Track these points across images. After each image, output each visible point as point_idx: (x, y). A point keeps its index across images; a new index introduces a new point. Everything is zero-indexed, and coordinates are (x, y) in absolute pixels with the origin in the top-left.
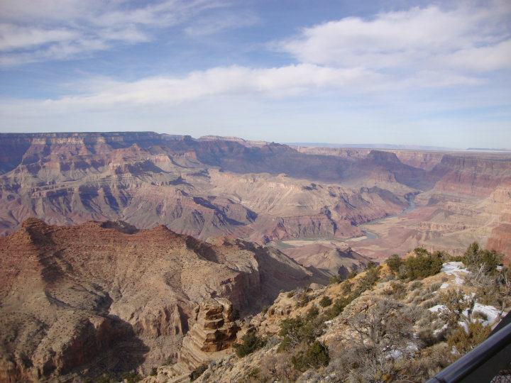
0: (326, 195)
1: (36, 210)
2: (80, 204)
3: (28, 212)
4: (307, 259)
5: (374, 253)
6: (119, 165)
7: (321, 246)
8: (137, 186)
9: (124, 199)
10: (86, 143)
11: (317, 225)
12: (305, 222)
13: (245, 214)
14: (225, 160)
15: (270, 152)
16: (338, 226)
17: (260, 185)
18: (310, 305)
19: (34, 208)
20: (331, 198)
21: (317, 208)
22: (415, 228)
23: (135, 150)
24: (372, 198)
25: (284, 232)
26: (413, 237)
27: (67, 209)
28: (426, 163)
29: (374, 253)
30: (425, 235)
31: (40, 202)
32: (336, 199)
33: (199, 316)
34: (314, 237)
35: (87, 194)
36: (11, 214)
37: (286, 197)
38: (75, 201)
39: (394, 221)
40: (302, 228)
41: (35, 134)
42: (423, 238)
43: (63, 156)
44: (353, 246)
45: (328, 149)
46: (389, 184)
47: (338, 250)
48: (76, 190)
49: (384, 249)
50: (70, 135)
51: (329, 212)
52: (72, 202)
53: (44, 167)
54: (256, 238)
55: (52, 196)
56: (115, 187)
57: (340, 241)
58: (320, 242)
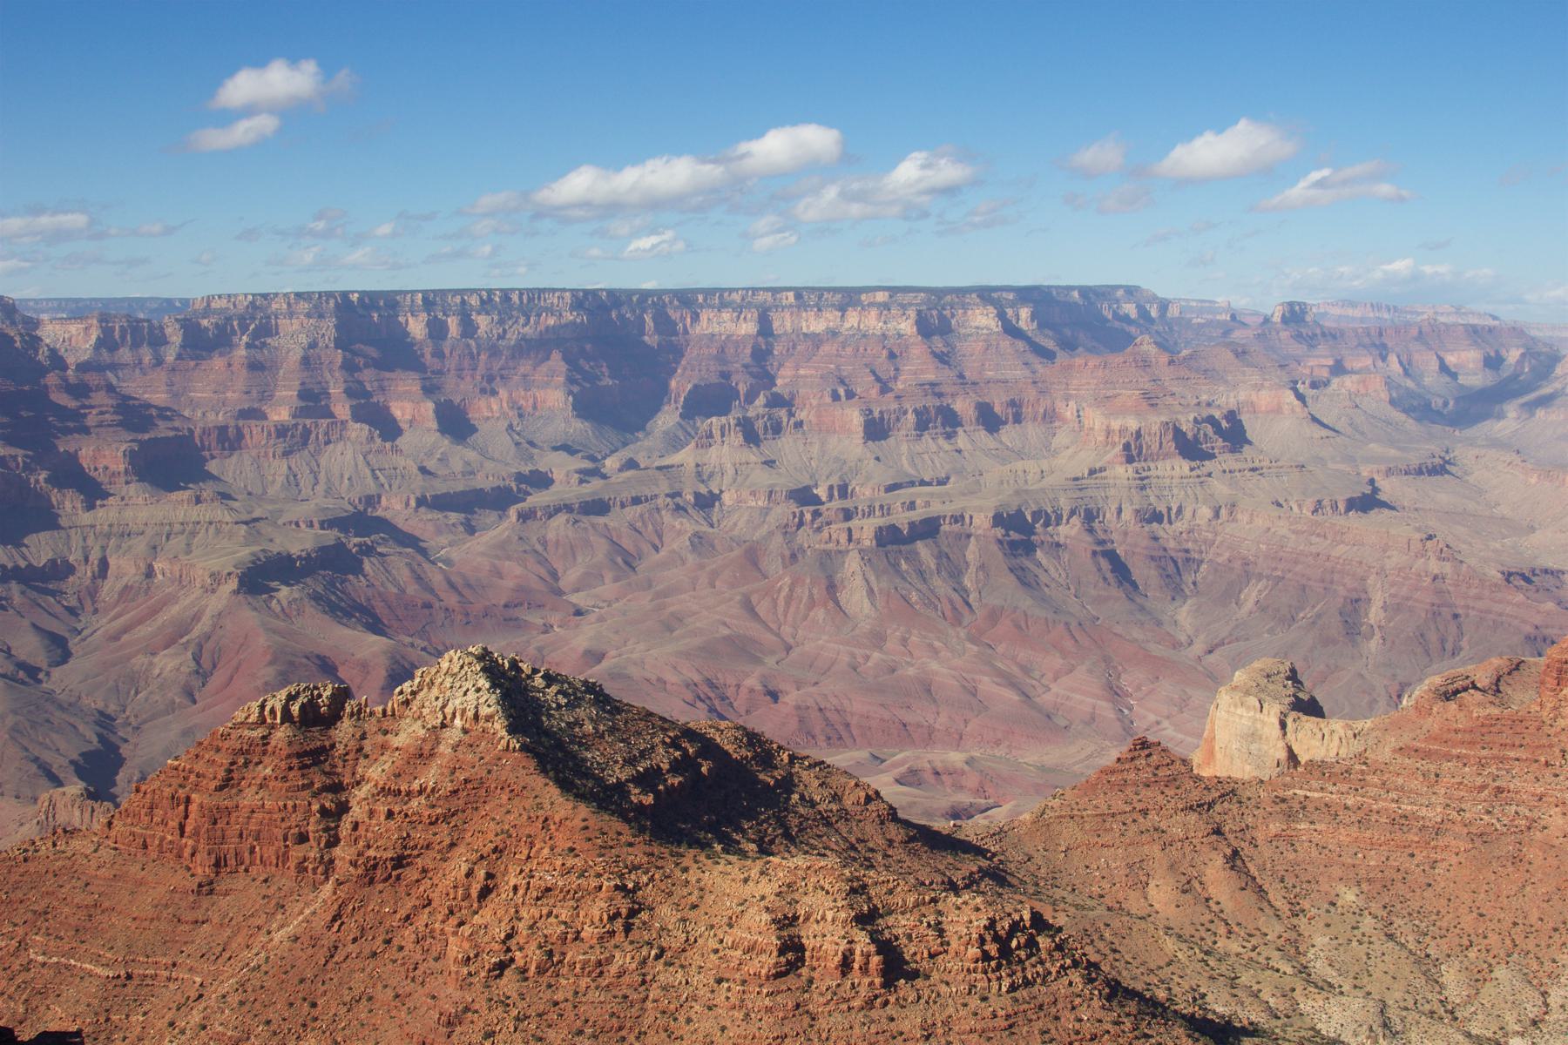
1: (843, 597)
2: (1010, 581)
3: (812, 604)
6: (1133, 424)
8: (1217, 515)
9: (1171, 569)
10: (925, 328)
19: (832, 588)
23: (1145, 364)
27: (955, 596)
31: (853, 563)
35: (1019, 532)
36: (749, 608)
38: (982, 567)
41: (709, 292)
43: (842, 382)
48: (981, 521)
50: (849, 298)
52: (972, 569)
53: (799, 425)
55: (889, 537)
56: (1127, 514)
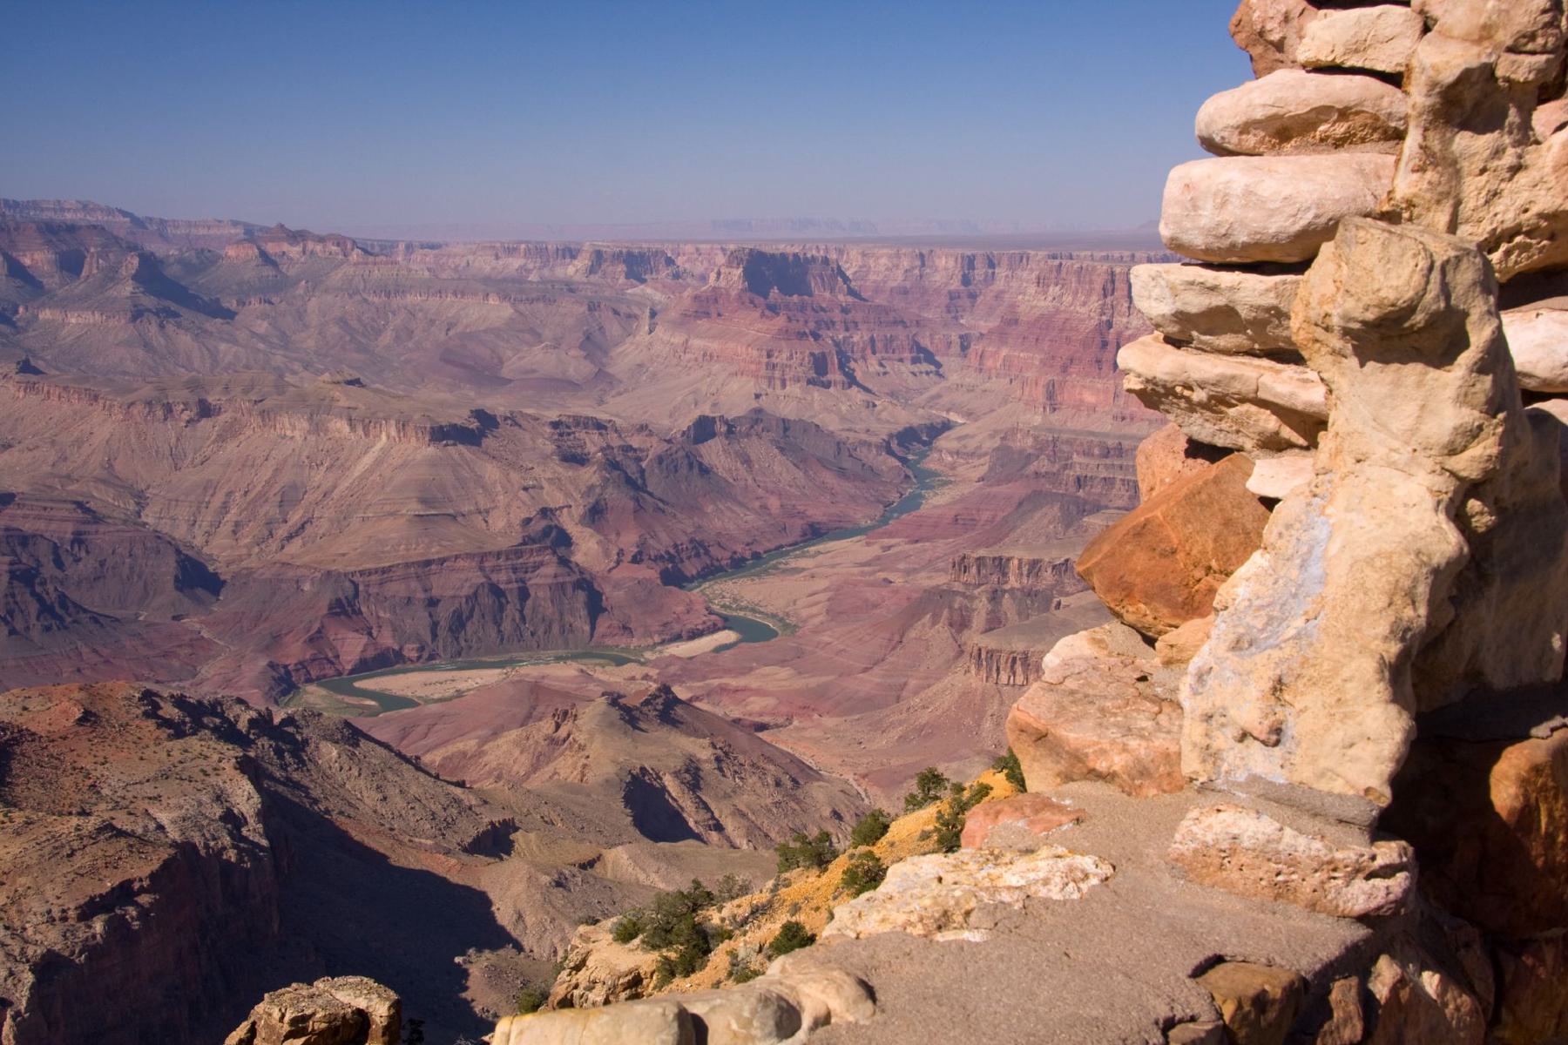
0: (546, 458)
4: (480, 754)
5: (771, 701)
7: (537, 690)
11: (513, 598)
12: (457, 583)
13: (168, 567)
14: (46, 315)
15: (268, 272)
16: (613, 595)
17: (230, 432)
20: (565, 472)
21: (503, 523)
22: (941, 580)
24: (747, 461)
25: (365, 639)
26: (934, 623)
28: (973, 296)
29: (771, 702)
30: (982, 606)
32: (589, 475)
34: (502, 650)
37: (362, 477)
39: (843, 557)
40: (444, 613)
42: (978, 621)
44: (679, 678)
45: (539, 251)
46: (817, 394)
47: (615, 700)
49: (813, 682)
51: (564, 540)
54: (232, 676)
57: (620, 662)
58: (529, 672)
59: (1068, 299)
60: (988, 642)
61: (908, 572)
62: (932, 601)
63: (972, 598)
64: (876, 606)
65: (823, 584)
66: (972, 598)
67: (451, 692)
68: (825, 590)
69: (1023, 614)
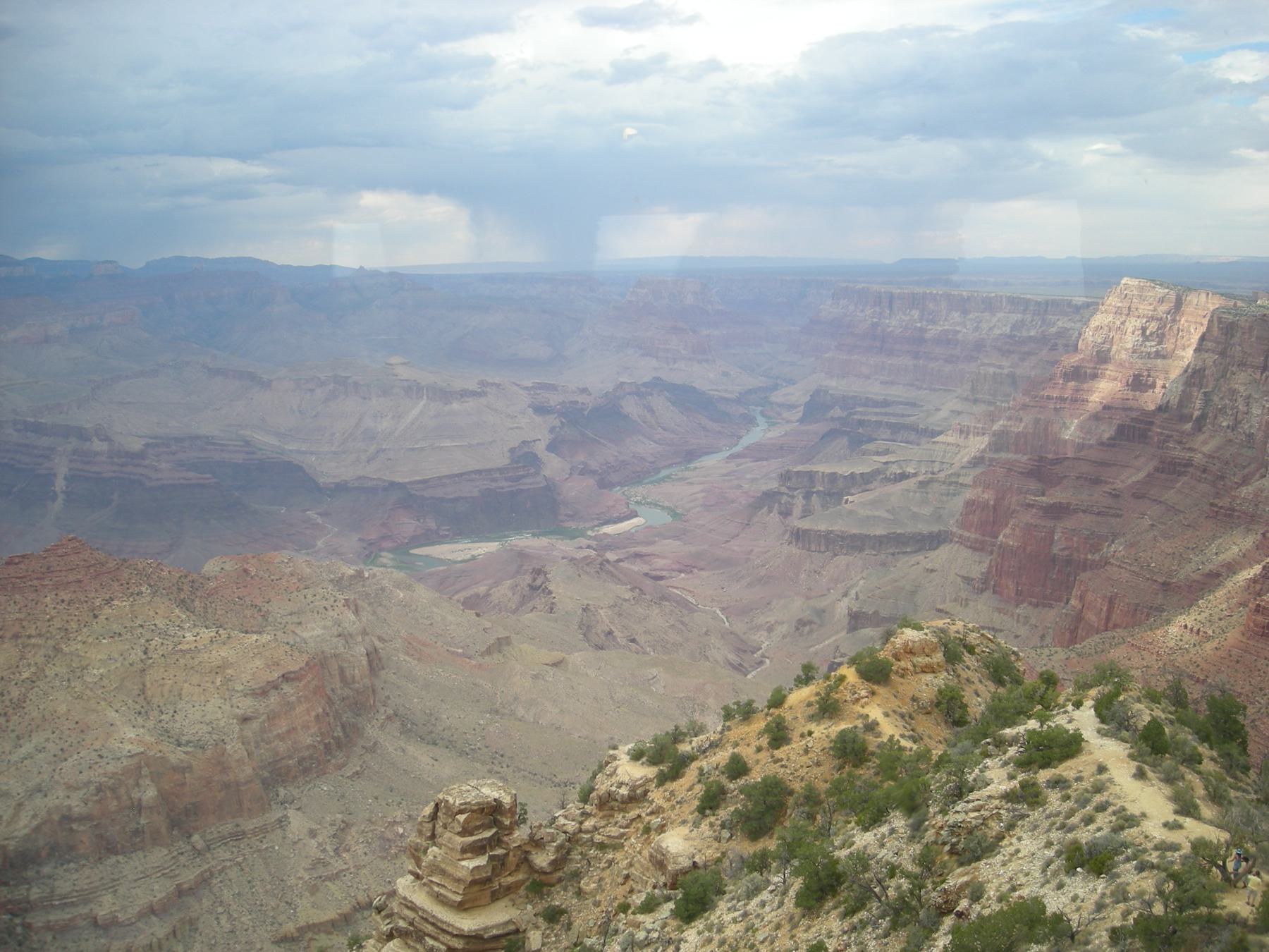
18: (691, 773)
20: (538, 419)
22: (773, 485)
26: (770, 512)
30: (799, 502)
33: (439, 830)
42: (797, 511)
59: (851, 308)
60: (805, 524)
61: (754, 480)
62: (769, 497)
63: (793, 497)
64: (733, 502)
65: (701, 487)
66: (793, 497)
67: (468, 556)
68: (702, 491)
69: (825, 506)
